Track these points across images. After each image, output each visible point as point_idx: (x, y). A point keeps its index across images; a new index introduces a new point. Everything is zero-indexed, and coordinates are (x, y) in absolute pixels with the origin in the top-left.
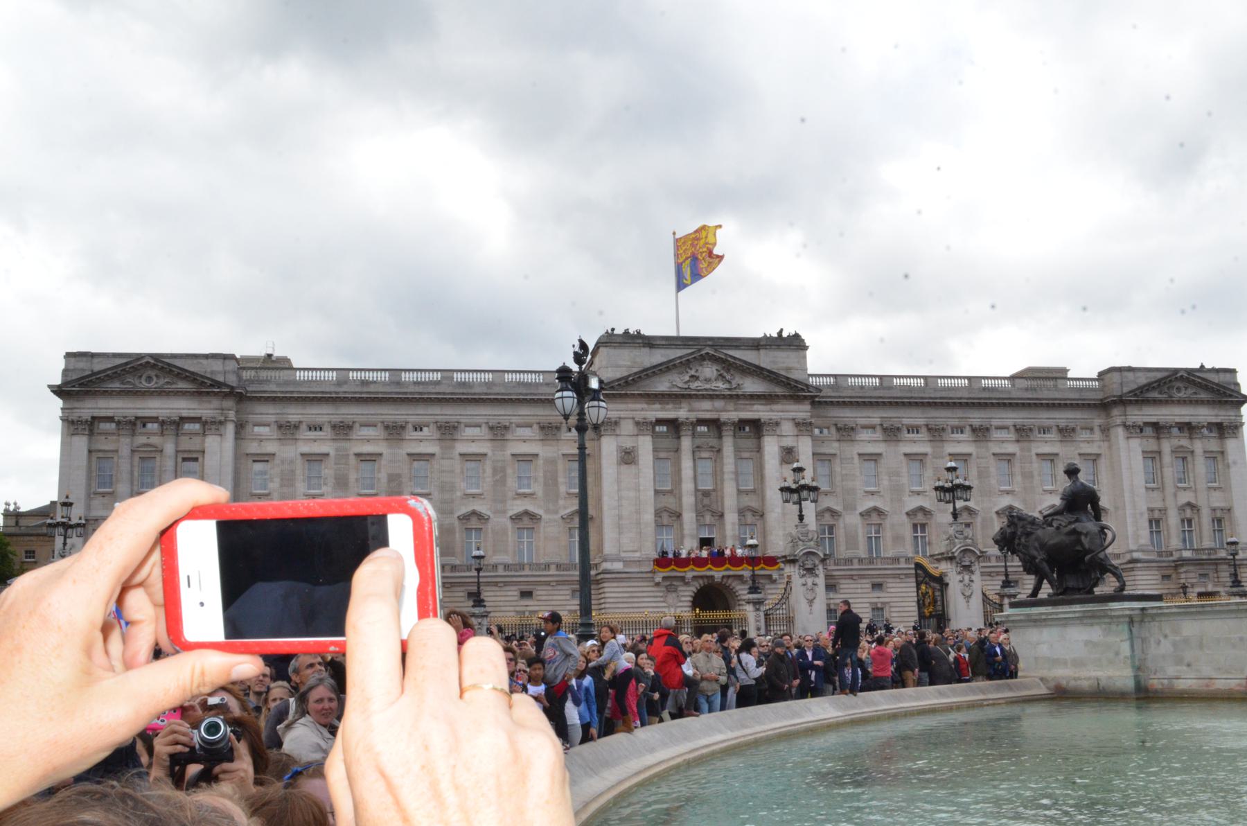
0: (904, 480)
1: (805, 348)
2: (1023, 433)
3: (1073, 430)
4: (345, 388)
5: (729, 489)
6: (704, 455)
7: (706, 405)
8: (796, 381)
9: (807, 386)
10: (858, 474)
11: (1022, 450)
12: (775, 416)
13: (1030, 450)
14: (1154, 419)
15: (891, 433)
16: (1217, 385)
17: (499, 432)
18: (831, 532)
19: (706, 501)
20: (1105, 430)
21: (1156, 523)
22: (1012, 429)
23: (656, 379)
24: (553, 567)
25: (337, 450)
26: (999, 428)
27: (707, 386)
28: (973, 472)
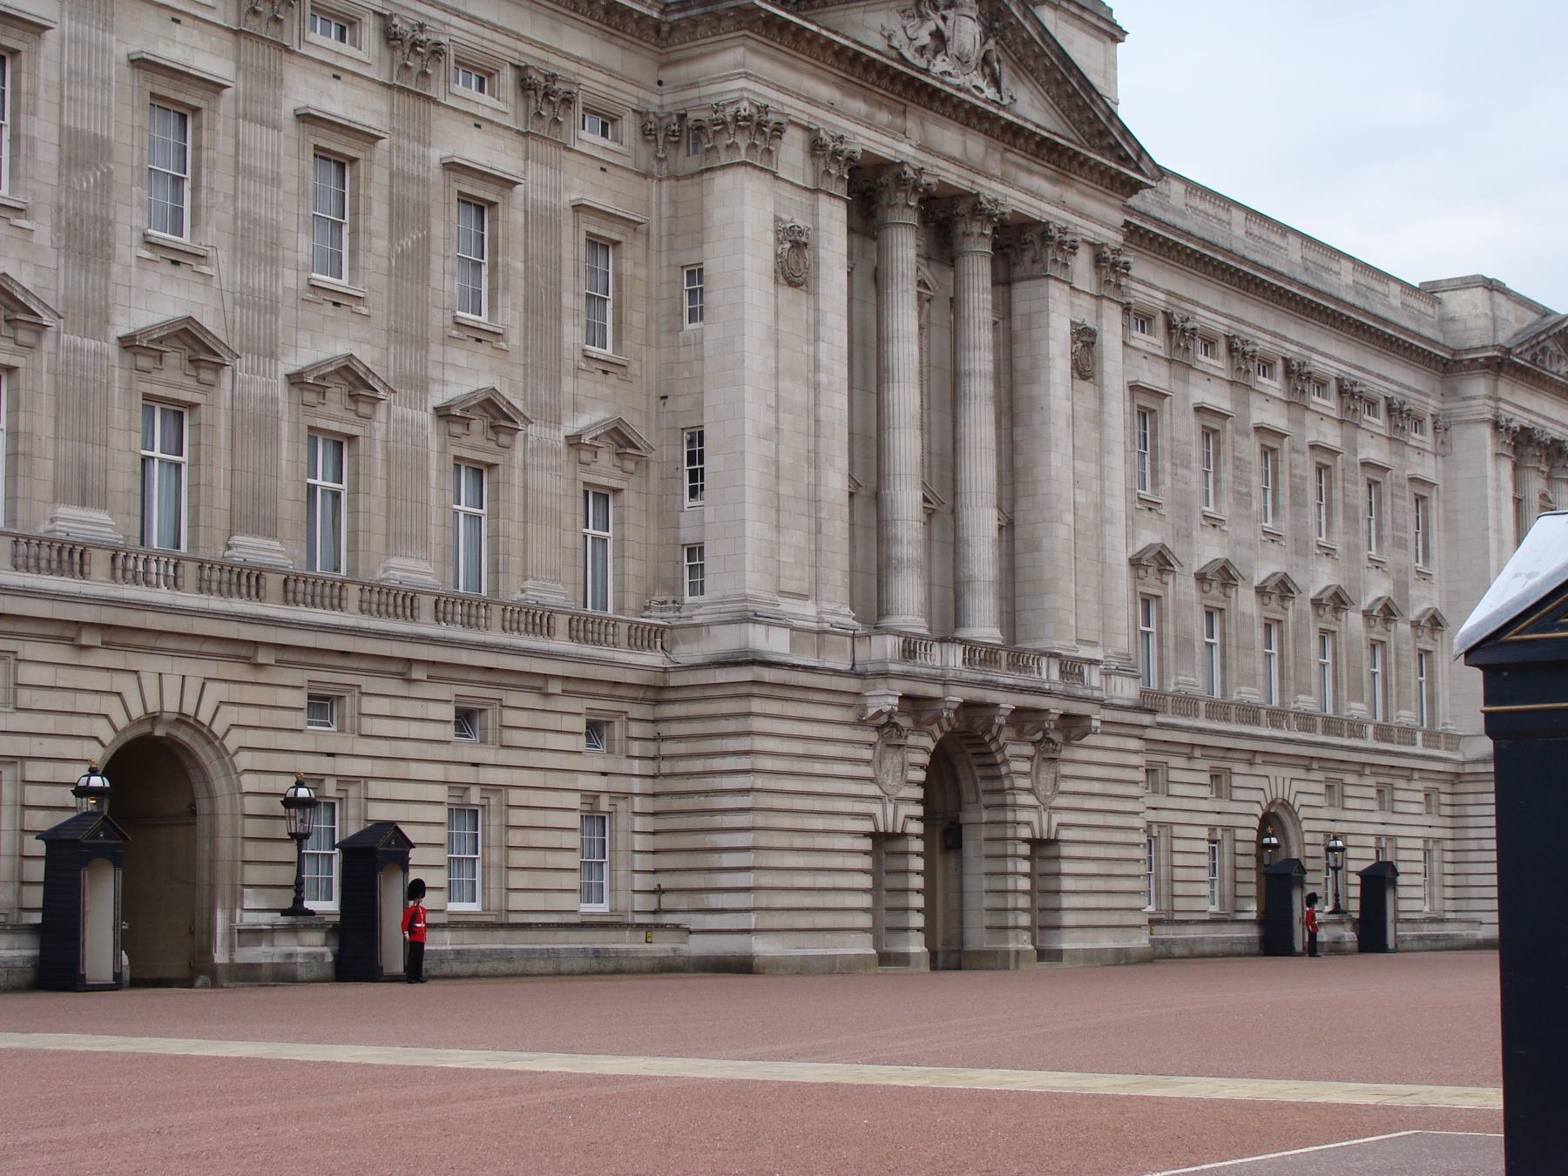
0: (1194, 478)
7: (951, 137)
13: (1355, 453)
20: (1441, 427)
22: (1333, 385)
24: (561, 622)
28: (1285, 490)
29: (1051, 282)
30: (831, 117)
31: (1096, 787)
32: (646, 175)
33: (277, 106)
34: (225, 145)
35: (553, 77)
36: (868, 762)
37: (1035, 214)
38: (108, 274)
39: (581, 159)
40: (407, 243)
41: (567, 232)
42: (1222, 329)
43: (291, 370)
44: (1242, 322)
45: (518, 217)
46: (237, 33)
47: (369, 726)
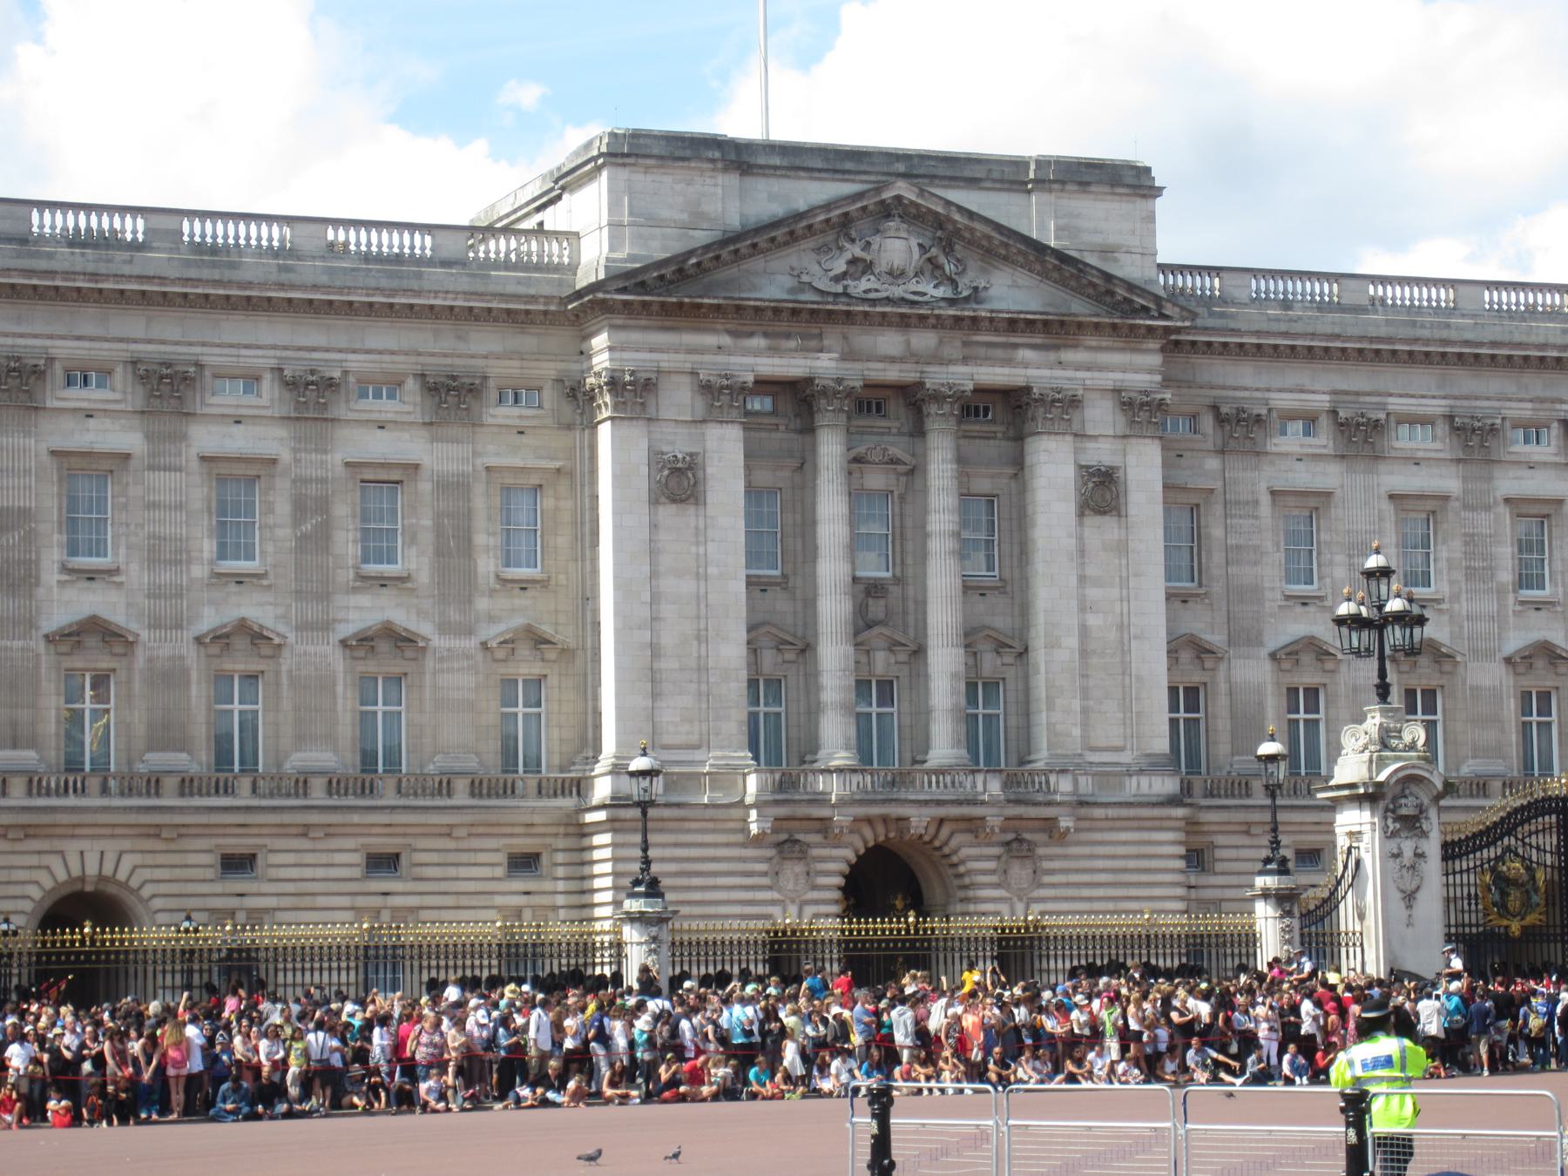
1: (1153, 192)
5: (941, 582)
6: (876, 479)
7: (889, 341)
8: (1130, 286)
9: (1157, 299)
10: (1269, 545)
15: (1361, 435)
17: (312, 395)
18: (1192, 706)
19: (876, 609)
23: (757, 264)
24: (461, 785)
27: (897, 291)
29: (1045, 437)
30: (721, 359)
31: (1103, 878)
32: (570, 427)
33: (180, 455)
34: (135, 491)
35: (454, 378)
36: (765, 874)
39: (496, 430)
40: (307, 527)
41: (479, 490)
42: (1440, 411)
43: (197, 634)
44: (1477, 398)
45: (425, 487)
46: (143, 412)
47: (273, 873)
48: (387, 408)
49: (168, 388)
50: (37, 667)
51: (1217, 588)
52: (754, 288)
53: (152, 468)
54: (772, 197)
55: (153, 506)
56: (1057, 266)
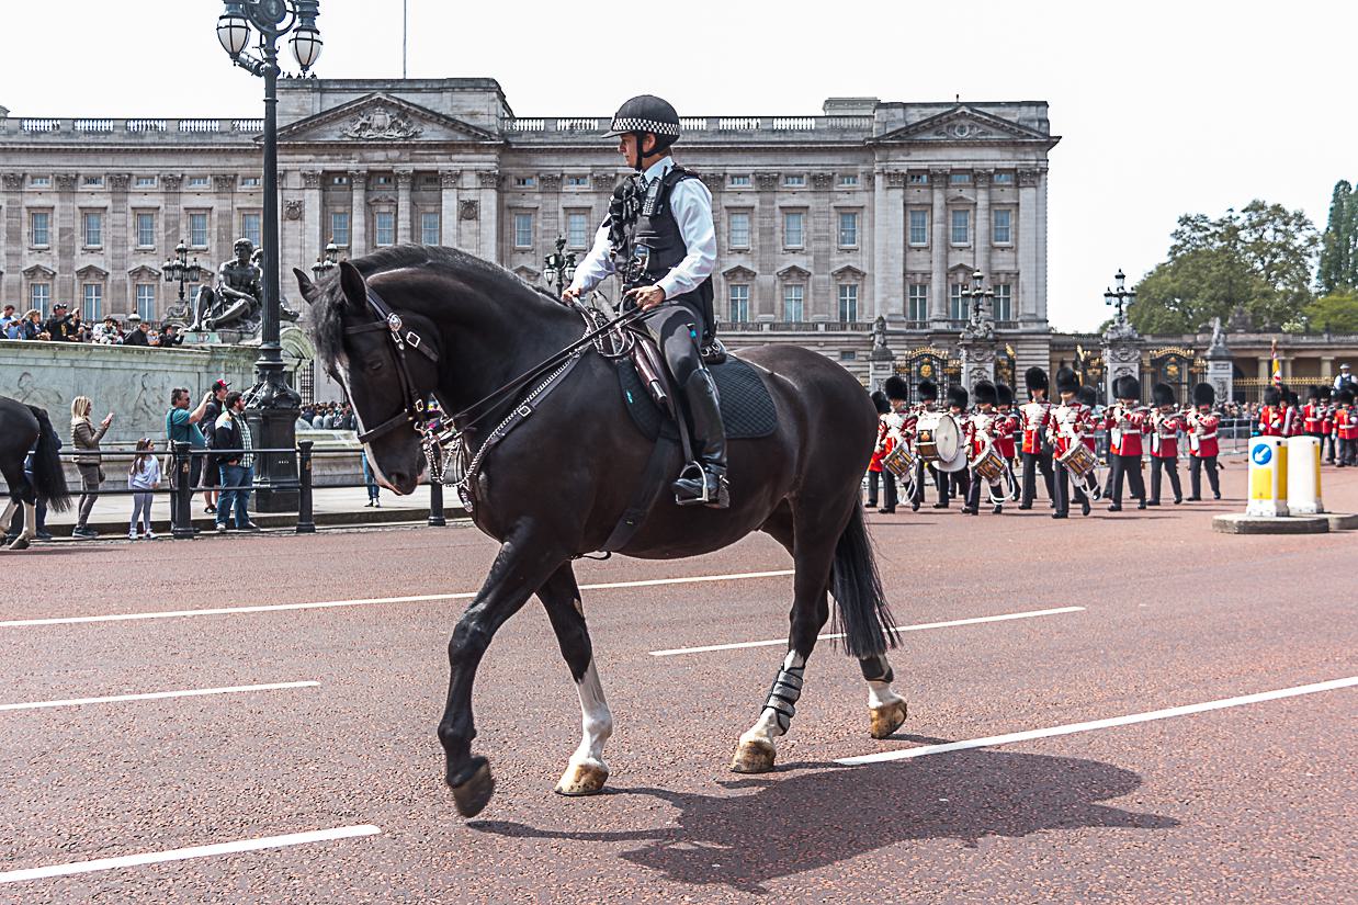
2: (766, 183)
3: (830, 179)
4: (14, 139)
6: (385, 209)
7: (379, 155)
8: (476, 128)
11: (761, 203)
12: (455, 167)
13: (773, 203)
14: (924, 166)
16: (1009, 122)
17: (173, 184)
21: (915, 286)
25: (8, 203)
26: (733, 177)
27: (380, 135)
30: (311, 164)
37: (435, 168)
38: (72, 259)
45: (215, 216)
48: (199, 186)
49: (120, 183)
50: (73, 284)
51: (539, 247)
52: (325, 137)
53: (114, 212)
54: (336, 101)
55: (114, 226)
56: (448, 122)
